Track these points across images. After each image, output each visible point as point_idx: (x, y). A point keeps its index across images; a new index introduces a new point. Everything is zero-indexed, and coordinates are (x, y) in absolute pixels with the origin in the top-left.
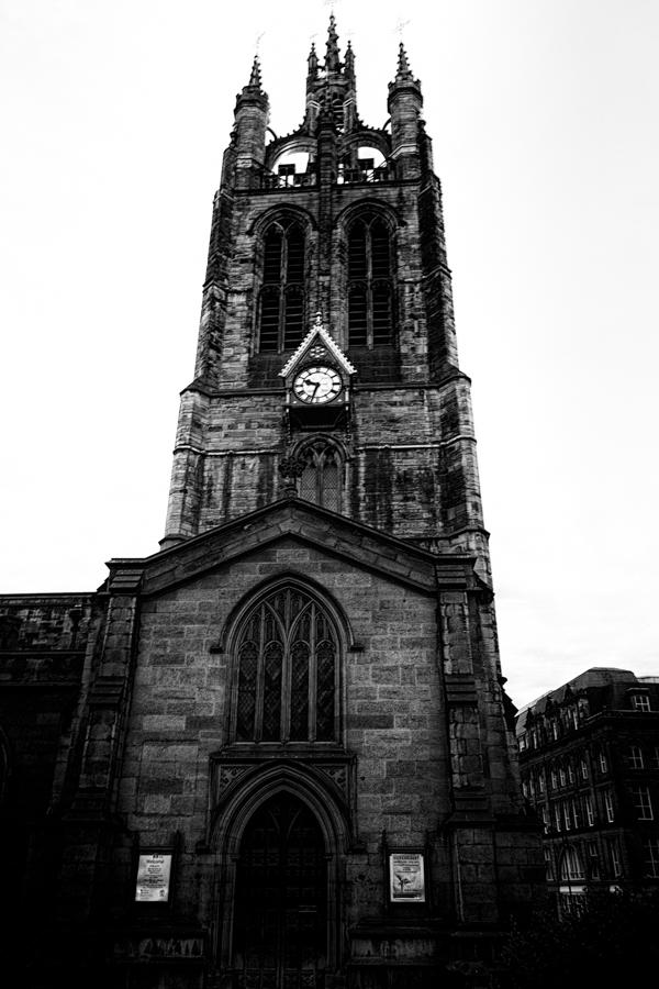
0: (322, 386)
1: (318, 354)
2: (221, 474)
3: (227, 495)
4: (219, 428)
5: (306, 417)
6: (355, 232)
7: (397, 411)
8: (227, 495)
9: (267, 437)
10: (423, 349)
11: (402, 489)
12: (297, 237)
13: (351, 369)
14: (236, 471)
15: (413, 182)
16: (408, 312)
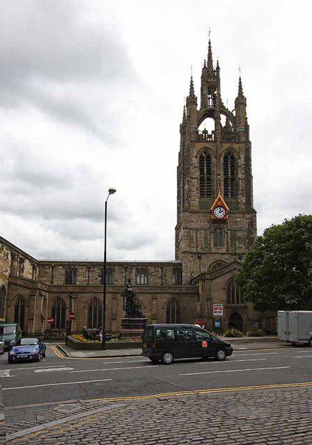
0: (219, 214)
2: (195, 235)
3: (197, 240)
4: (193, 222)
5: (216, 221)
6: (225, 157)
7: (238, 219)
8: (197, 240)
9: (206, 225)
10: (244, 201)
11: (238, 241)
12: (209, 157)
13: (228, 209)
14: (198, 233)
15: (244, 142)
16: (241, 188)
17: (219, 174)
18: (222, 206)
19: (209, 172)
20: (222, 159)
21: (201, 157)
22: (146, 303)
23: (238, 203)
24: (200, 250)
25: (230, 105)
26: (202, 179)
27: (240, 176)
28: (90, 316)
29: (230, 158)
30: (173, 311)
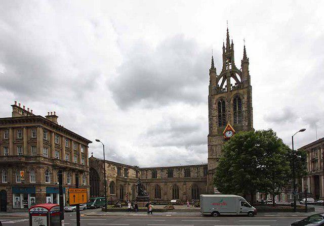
1: (229, 129)
6: (235, 100)
10: (247, 124)
17: (230, 110)
18: (231, 130)
19: (224, 111)
20: (232, 102)
21: (219, 103)
22: (181, 187)
23: (242, 126)
24: (218, 157)
25: (238, 65)
26: (219, 116)
27: (244, 109)
28: (156, 193)
29: (238, 100)
30: (195, 190)
